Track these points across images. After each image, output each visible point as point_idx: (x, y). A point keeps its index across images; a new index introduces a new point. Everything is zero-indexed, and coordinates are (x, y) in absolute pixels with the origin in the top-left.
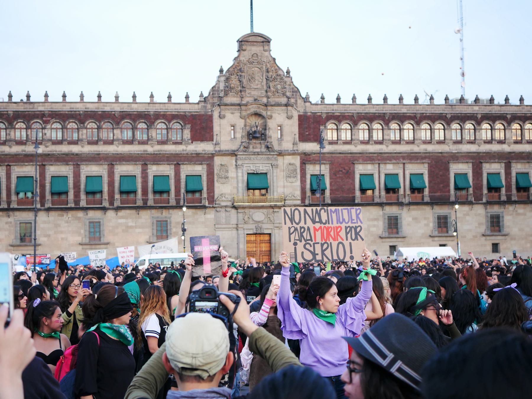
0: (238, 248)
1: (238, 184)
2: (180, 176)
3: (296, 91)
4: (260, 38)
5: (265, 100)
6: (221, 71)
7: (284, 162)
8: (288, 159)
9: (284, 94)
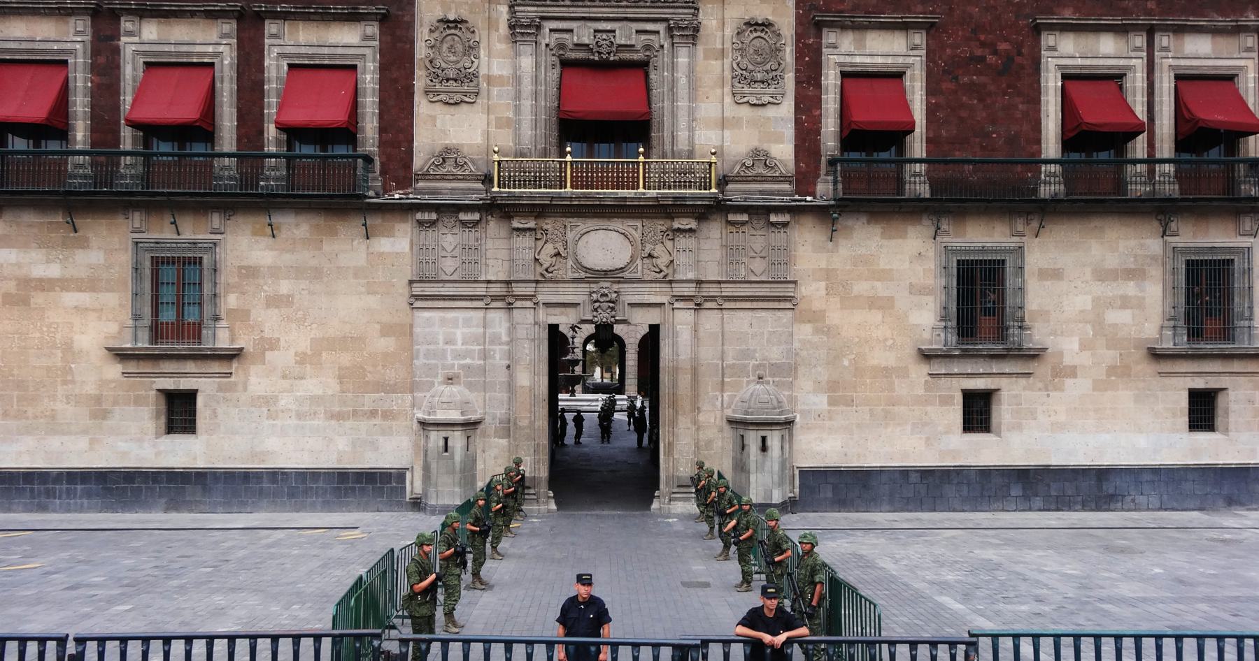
0: (511, 387)
1: (517, 110)
2: (261, 68)
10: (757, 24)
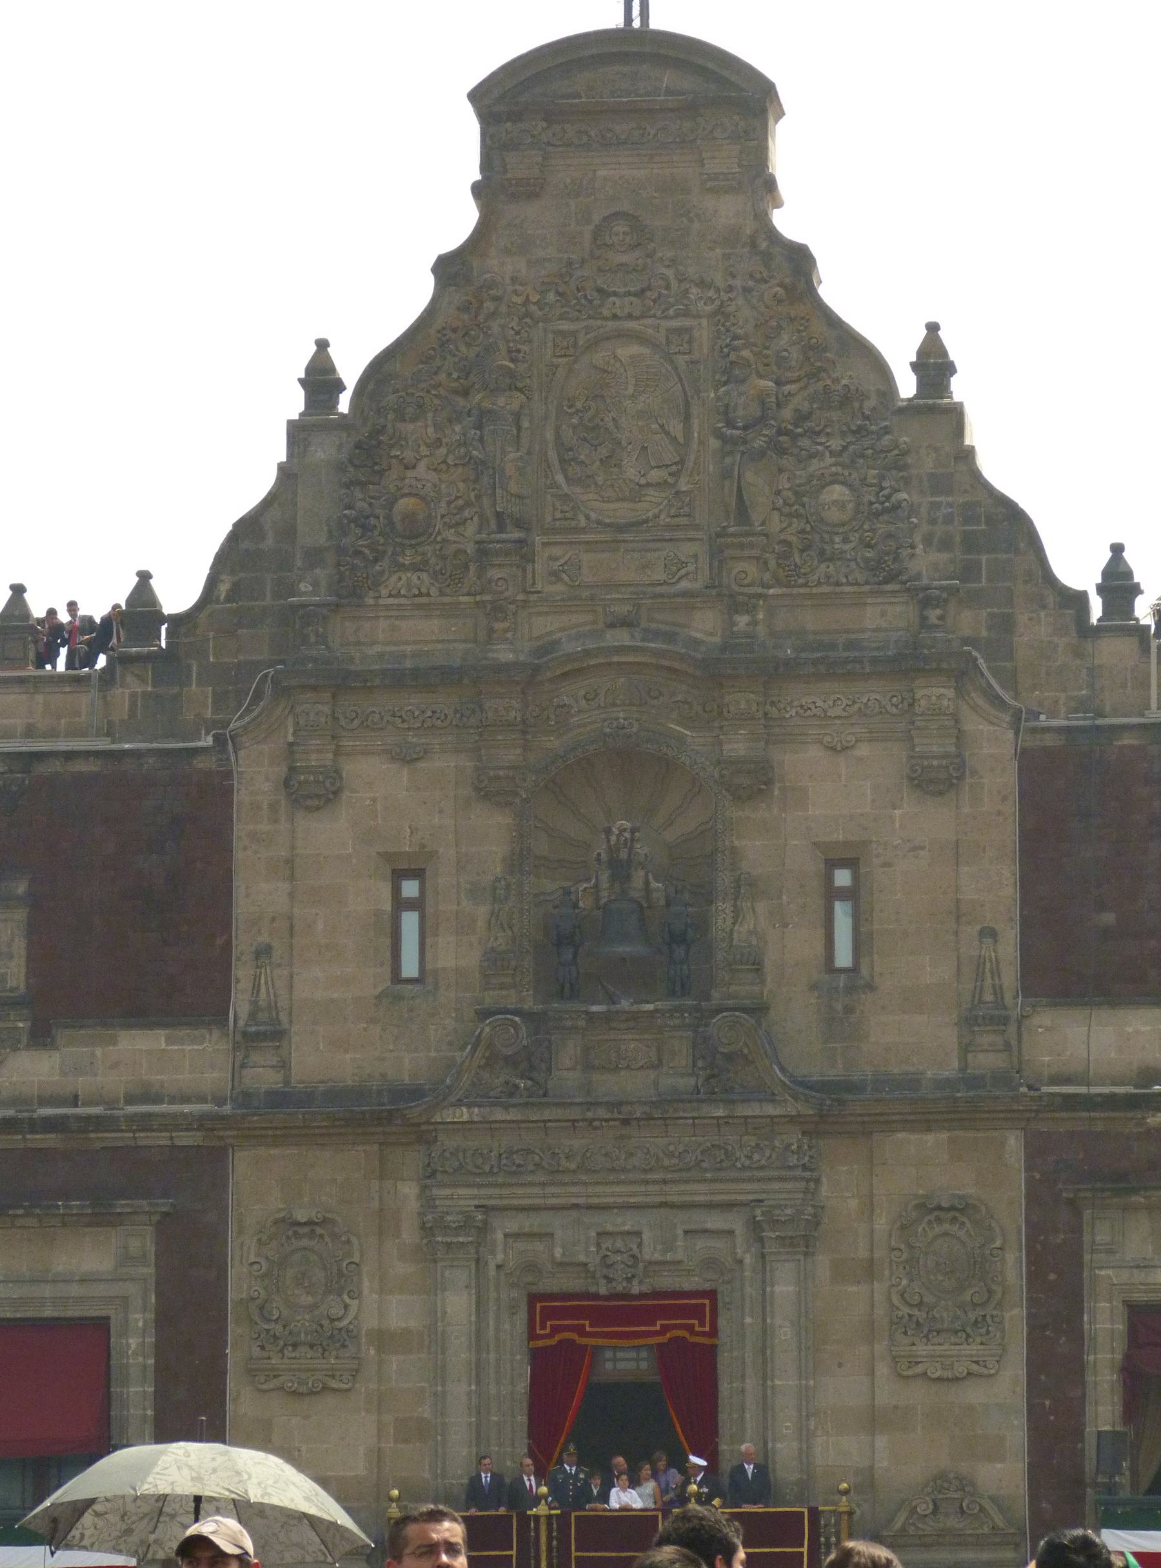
3: (1009, 528)
4: (668, 78)
5: (705, 626)
6: (320, 379)
7: (870, 1191)
8: (921, 1163)
9: (886, 572)
10: (939, 1208)
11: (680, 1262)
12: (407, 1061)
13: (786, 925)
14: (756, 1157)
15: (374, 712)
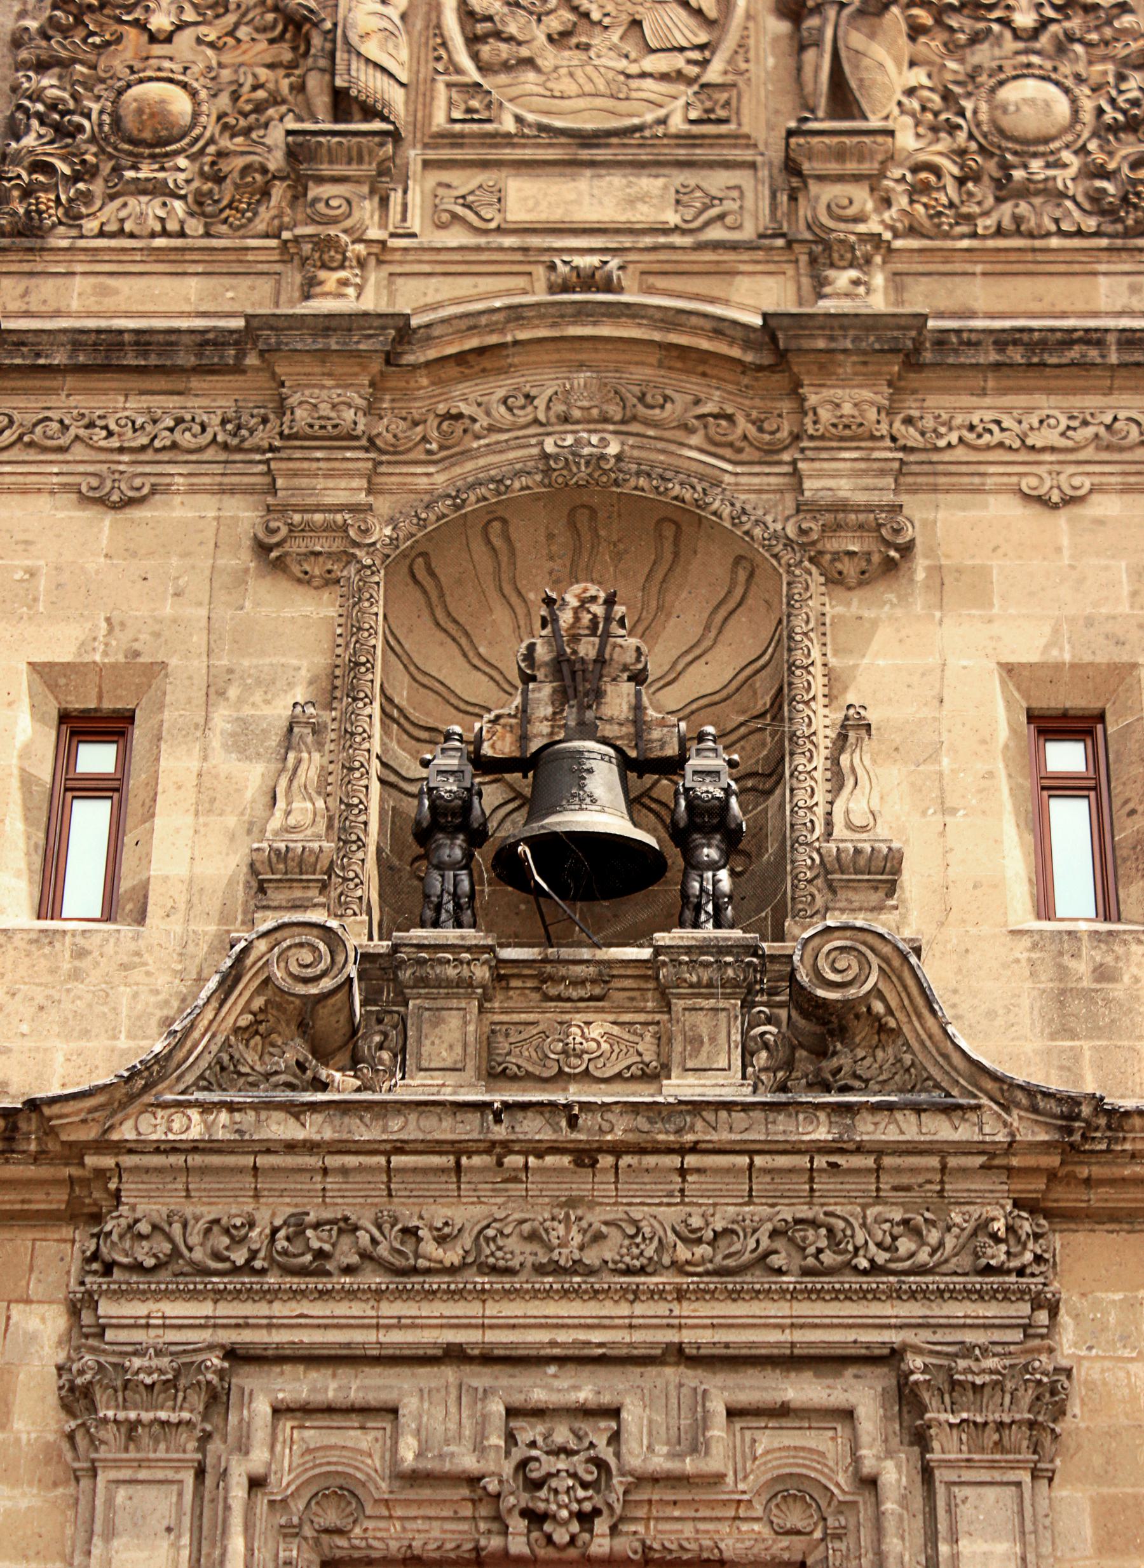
5: (756, 297)
11: (720, 1477)
12: (60, 1058)
13: (947, 810)
14: (905, 1245)
15: (48, 419)
